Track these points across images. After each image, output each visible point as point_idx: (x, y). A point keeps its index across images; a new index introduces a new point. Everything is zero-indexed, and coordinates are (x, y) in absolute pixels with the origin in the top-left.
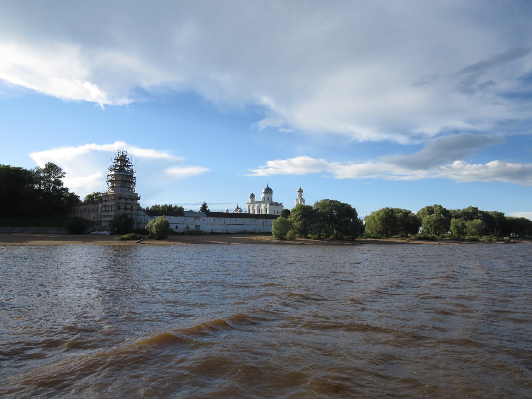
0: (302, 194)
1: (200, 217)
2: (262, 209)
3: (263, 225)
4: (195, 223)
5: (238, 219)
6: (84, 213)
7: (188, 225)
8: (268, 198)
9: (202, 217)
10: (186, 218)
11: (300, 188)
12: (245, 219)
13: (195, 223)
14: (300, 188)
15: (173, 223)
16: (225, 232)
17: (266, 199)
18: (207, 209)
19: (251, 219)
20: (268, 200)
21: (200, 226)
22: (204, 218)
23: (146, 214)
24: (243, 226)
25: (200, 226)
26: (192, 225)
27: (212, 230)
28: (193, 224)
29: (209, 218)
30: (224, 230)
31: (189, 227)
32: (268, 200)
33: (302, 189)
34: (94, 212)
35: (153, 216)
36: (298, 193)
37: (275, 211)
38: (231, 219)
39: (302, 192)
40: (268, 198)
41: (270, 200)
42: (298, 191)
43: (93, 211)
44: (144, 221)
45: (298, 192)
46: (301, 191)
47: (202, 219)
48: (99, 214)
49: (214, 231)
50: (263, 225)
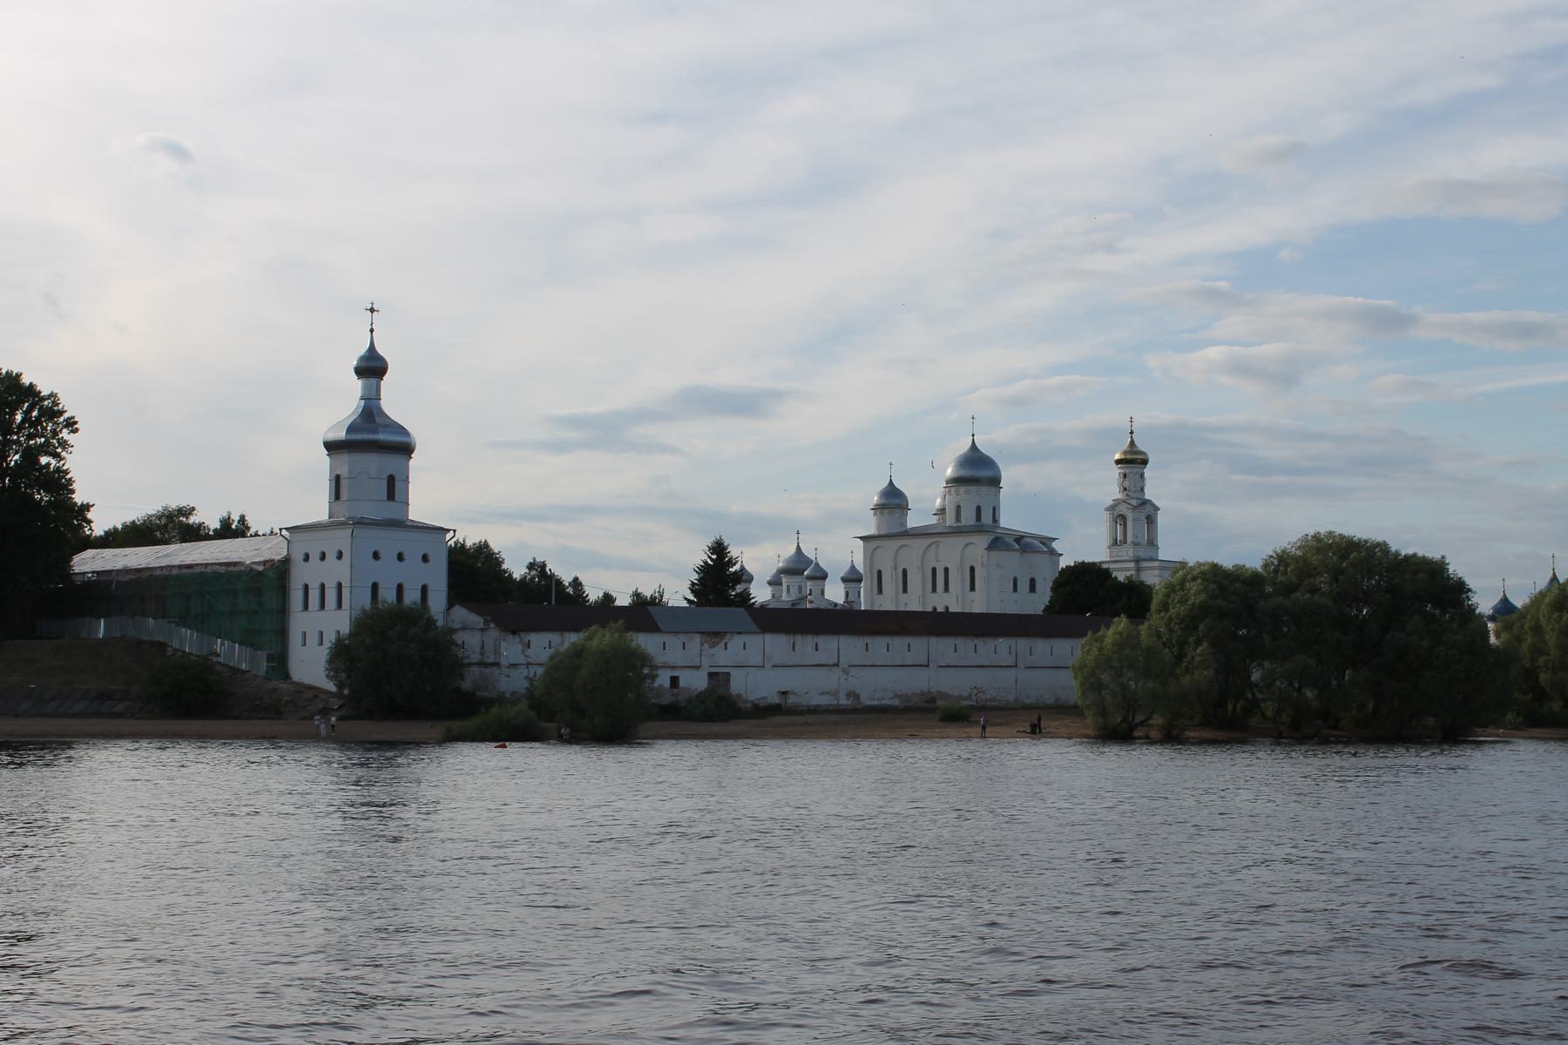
0: (1142, 476)
1: (729, 636)
2: (946, 570)
3: (1016, 666)
4: (706, 662)
5: (899, 643)
7: (675, 673)
8: (979, 509)
9: (739, 633)
10: (668, 639)
11: (1132, 442)
12: (933, 640)
13: (706, 662)
14: (1132, 442)
16: (844, 701)
17: (968, 518)
19: (960, 641)
20: (978, 517)
21: (728, 674)
22: (748, 639)
23: (492, 625)
25: (728, 674)
26: (693, 672)
27: (784, 693)
28: (697, 668)
29: (769, 637)
30: (836, 694)
31: (682, 683)
32: (978, 517)
33: (1141, 446)
35: (522, 635)
37: (1015, 581)
38: (869, 640)
39: (1145, 462)
40: (979, 509)
41: (986, 518)
42: (1117, 456)
44: (482, 654)
45: (1118, 462)
47: (736, 642)
49: (792, 700)
50: (1016, 666)
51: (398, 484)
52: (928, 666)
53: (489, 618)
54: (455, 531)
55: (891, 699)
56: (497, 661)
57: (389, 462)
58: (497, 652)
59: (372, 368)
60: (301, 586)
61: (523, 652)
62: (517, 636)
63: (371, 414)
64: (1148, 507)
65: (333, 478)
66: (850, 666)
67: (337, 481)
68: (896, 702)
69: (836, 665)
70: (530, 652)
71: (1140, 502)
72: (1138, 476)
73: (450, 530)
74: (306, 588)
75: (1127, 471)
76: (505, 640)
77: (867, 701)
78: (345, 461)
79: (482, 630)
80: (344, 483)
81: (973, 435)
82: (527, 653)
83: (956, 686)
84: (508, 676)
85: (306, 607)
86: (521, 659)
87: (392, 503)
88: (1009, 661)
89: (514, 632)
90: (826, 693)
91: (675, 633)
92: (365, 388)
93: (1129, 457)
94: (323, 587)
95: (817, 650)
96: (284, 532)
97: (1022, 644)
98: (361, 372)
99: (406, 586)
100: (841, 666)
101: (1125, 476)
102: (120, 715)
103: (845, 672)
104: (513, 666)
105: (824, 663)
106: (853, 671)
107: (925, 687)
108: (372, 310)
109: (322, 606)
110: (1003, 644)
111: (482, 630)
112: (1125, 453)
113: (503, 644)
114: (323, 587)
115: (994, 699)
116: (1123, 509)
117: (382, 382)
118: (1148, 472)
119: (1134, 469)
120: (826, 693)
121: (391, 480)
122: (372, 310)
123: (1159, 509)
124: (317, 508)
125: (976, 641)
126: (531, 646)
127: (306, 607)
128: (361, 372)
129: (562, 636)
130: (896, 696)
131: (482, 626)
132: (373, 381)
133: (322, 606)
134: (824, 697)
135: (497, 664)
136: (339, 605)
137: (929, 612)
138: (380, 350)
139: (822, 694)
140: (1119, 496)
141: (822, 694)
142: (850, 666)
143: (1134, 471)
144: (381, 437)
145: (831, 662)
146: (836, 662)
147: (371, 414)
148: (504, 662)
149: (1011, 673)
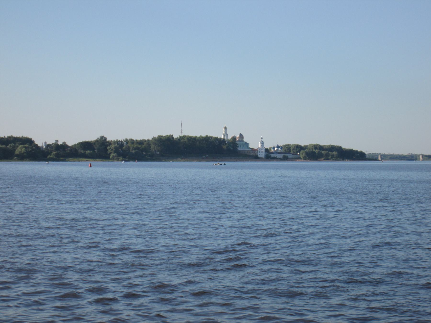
33: (226, 127)
43: (252, 152)
46: (226, 128)
48: (256, 154)
59: (262, 138)
63: (262, 141)
78: (262, 144)
118: (227, 130)
147: (262, 141)
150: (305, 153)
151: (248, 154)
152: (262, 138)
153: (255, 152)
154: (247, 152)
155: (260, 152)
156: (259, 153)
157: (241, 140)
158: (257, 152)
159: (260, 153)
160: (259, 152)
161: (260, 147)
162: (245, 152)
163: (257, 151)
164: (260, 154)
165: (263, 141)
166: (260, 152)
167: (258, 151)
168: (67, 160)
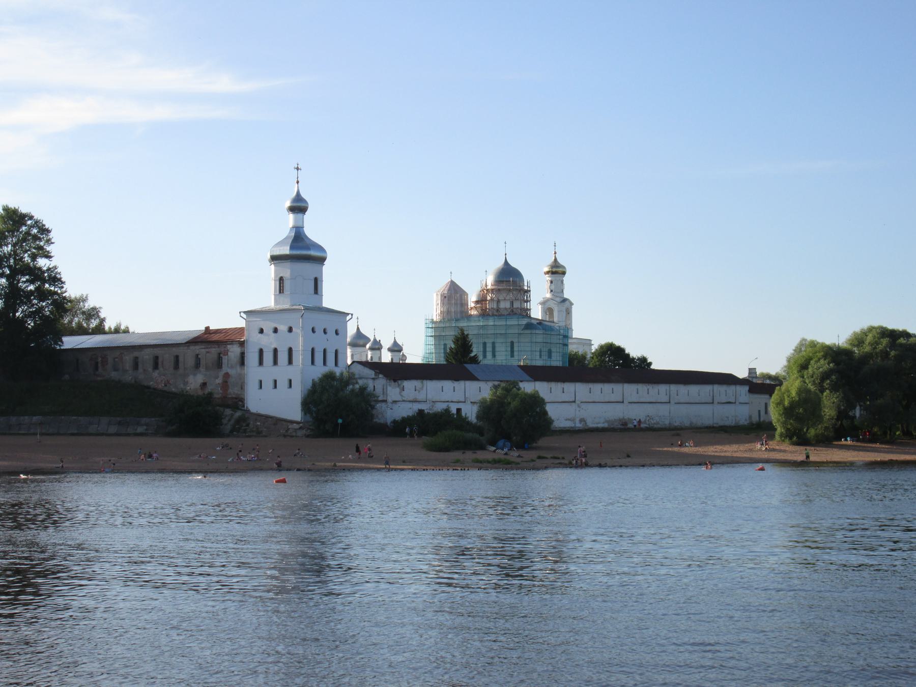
0: (562, 282)
6: (150, 370)
11: (556, 260)
12: (626, 386)
14: (556, 260)
15: (450, 400)
16: (579, 425)
18: (472, 355)
23: (381, 376)
24: (619, 407)
30: (573, 420)
34: (202, 369)
35: (400, 382)
36: (548, 278)
38: (591, 385)
39: (564, 273)
42: (547, 269)
43: (197, 365)
45: (547, 273)
48: (227, 375)
50: (670, 402)
51: (319, 282)
52: (623, 402)
53: (378, 371)
54: (352, 315)
55: (603, 423)
56: (385, 399)
57: (307, 268)
58: (384, 392)
59: (299, 207)
60: (257, 350)
61: (400, 393)
62: (396, 383)
63: (298, 238)
64: (567, 302)
65: (278, 278)
66: (582, 402)
67: (281, 280)
68: (606, 425)
69: (574, 402)
70: (404, 393)
71: (562, 299)
72: (559, 283)
73: (348, 314)
74: (261, 352)
75: (553, 279)
76: (390, 385)
77: (591, 425)
78: (287, 270)
79: (373, 379)
80: (287, 284)
81: (506, 254)
82: (402, 394)
83: (636, 413)
84: (391, 409)
85: (261, 363)
86: (398, 398)
87: (316, 295)
88: (666, 399)
89: (395, 381)
90: (569, 420)
91: (486, 381)
92: (296, 220)
93: (554, 270)
94: (275, 351)
95: (563, 392)
96: (243, 314)
97: (674, 388)
98: (292, 209)
99: (316, 350)
100: (577, 402)
101: (551, 282)
102: (141, 434)
103: (579, 406)
104: (395, 402)
105: (567, 400)
106: (583, 406)
107: (620, 415)
108: (298, 169)
109: (275, 362)
110: (663, 388)
111: (373, 379)
112: (552, 267)
113: (389, 388)
114: (275, 351)
115: (658, 423)
116: (552, 305)
117: (305, 216)
118: (566, 279)
119: (557, 277)
120: (569, 420)
121: (316, 280)
122: (298, 169)
123: (573, 304)
124: (266, 298)
125: (649, 387)
126: (405, 390)
127: (261, 363)
128: (292, 209)
129: (422, 383)
130: (607, 421)
131: (373, 376)
132: (300, 215)
133: (275, 362)
134: (567, 421)
135: (385, 401)
136: (290, 362)
137: (557, 367)
138: (304, 195)
139: (566, 420)
140: (548, 295)
141: (566, 420)
142: (582, 402)
143: (558, 279)
144: (313, 253)
145: (571, 400)
146: (574, 399)
147: (298, 238)
148: (390, 399)
149: (667, 407)
150: (825, 365)
151: (157, 379)
152: (299, 207)
153: (219, 364)
154: (156, 366)
155: (268, 357)
156: (253, 372)
157: (504, 305)
158: (242, 362)
159: (268, 372)
160: (252, 358)
161: (266, 298)
162: (136, 365)
163: (235, 350)
164: (268, 384)
165: (312, 232)
166: (268, 357)
167: (242, 344)
168: (526, 445)
